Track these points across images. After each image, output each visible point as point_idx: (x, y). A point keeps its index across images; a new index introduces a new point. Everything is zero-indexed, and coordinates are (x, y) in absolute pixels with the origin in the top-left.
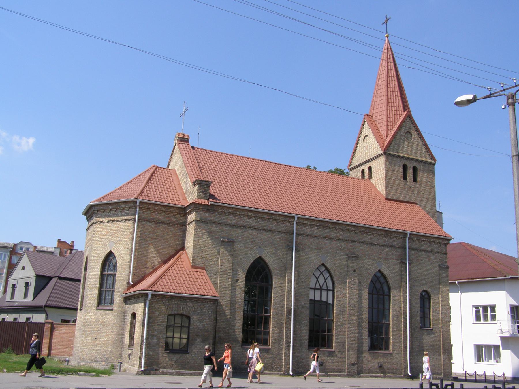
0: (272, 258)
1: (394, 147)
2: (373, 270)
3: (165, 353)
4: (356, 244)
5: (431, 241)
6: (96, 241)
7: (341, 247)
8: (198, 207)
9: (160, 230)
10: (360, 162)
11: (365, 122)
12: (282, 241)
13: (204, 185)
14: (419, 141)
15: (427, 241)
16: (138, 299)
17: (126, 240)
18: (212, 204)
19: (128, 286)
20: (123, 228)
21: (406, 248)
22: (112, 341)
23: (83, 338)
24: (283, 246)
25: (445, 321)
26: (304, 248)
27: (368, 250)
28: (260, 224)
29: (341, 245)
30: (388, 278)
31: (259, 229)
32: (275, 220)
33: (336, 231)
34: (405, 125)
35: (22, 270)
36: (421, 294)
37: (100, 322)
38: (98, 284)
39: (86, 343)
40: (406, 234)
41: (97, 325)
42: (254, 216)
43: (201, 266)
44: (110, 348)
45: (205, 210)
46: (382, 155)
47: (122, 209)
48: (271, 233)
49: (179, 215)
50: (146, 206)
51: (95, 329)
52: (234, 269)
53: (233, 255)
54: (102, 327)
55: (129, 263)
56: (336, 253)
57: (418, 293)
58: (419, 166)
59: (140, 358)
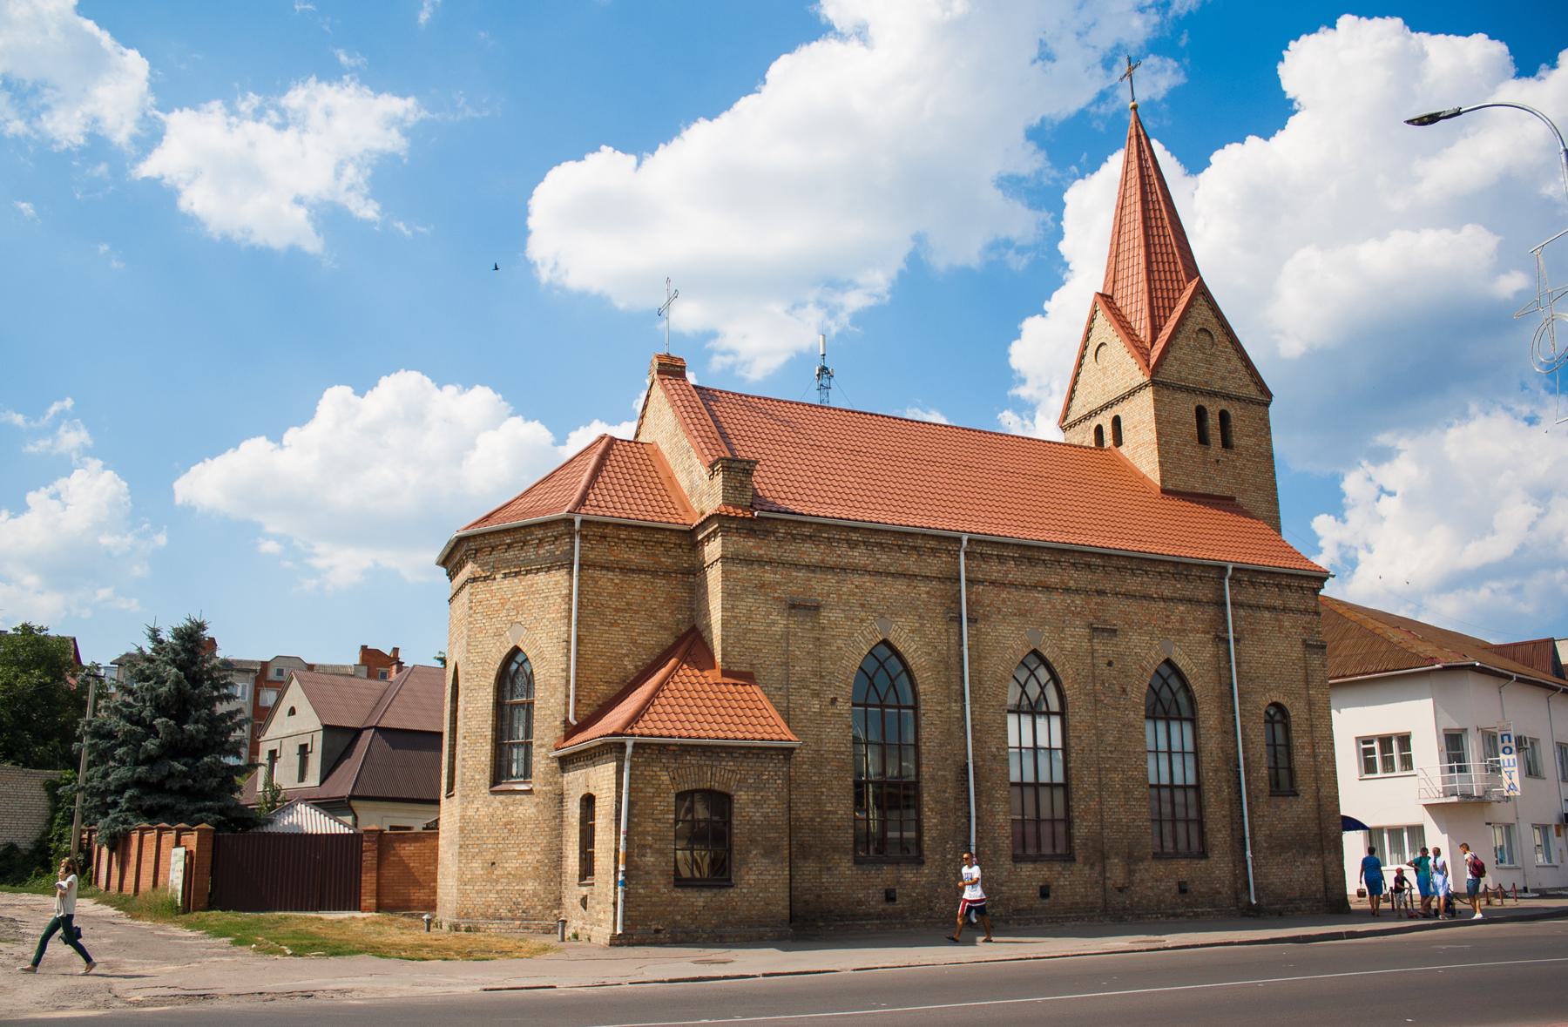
0: (913, 641)
1: (1171, 366)
2: (1153, 659)
3: (676, 889)
4: (1109, 599)
5: (1281, 584)
6: (478, 625)
7: (1073, 609)
8: (726, 525)
9: (635, 587)
10: (1089, 409)
11: (1096, 311)
12: (933, 600)
13: (737, 470)
14: (1230, 350)
15: (1274, 584)
16: (597, 759)
17: (553, 618)
18: (761, 515)
19: (565, 731)
20: (544, 587)
21: (1225, 604)
22: (533, 867)
23: (462, 865)
24: (937, 611)
26: (986, 613)
27: (1137, 611)
28: (878, 559)
29: (1073, 602)
30: (1188, 677)
31: (878, 573)
32: (914, 548)
33: (1060, 570)
34: (1194, 312)
35: (289, 715)
36: (1267, 712)
37: (501, 823)
38: (490, 729)
39: (469, 876)
40: (1224, 569)
41: (495, 831)
42: (864, 542)
43: (744, 669)
44: (530, 884)
45: (745, 531)
46: (1146, 386)
47: (537, 541)
48: (906, 580)
49: (680, 550)
50: (596, 530)
51: (491, 841)
52: (824, 674)
53: (819, 639)
54: (507, 835)
55: (565, 674)
56: (1064, 622)
57: (1260, 709)
58: (1234, 411)
59: (615, 904)
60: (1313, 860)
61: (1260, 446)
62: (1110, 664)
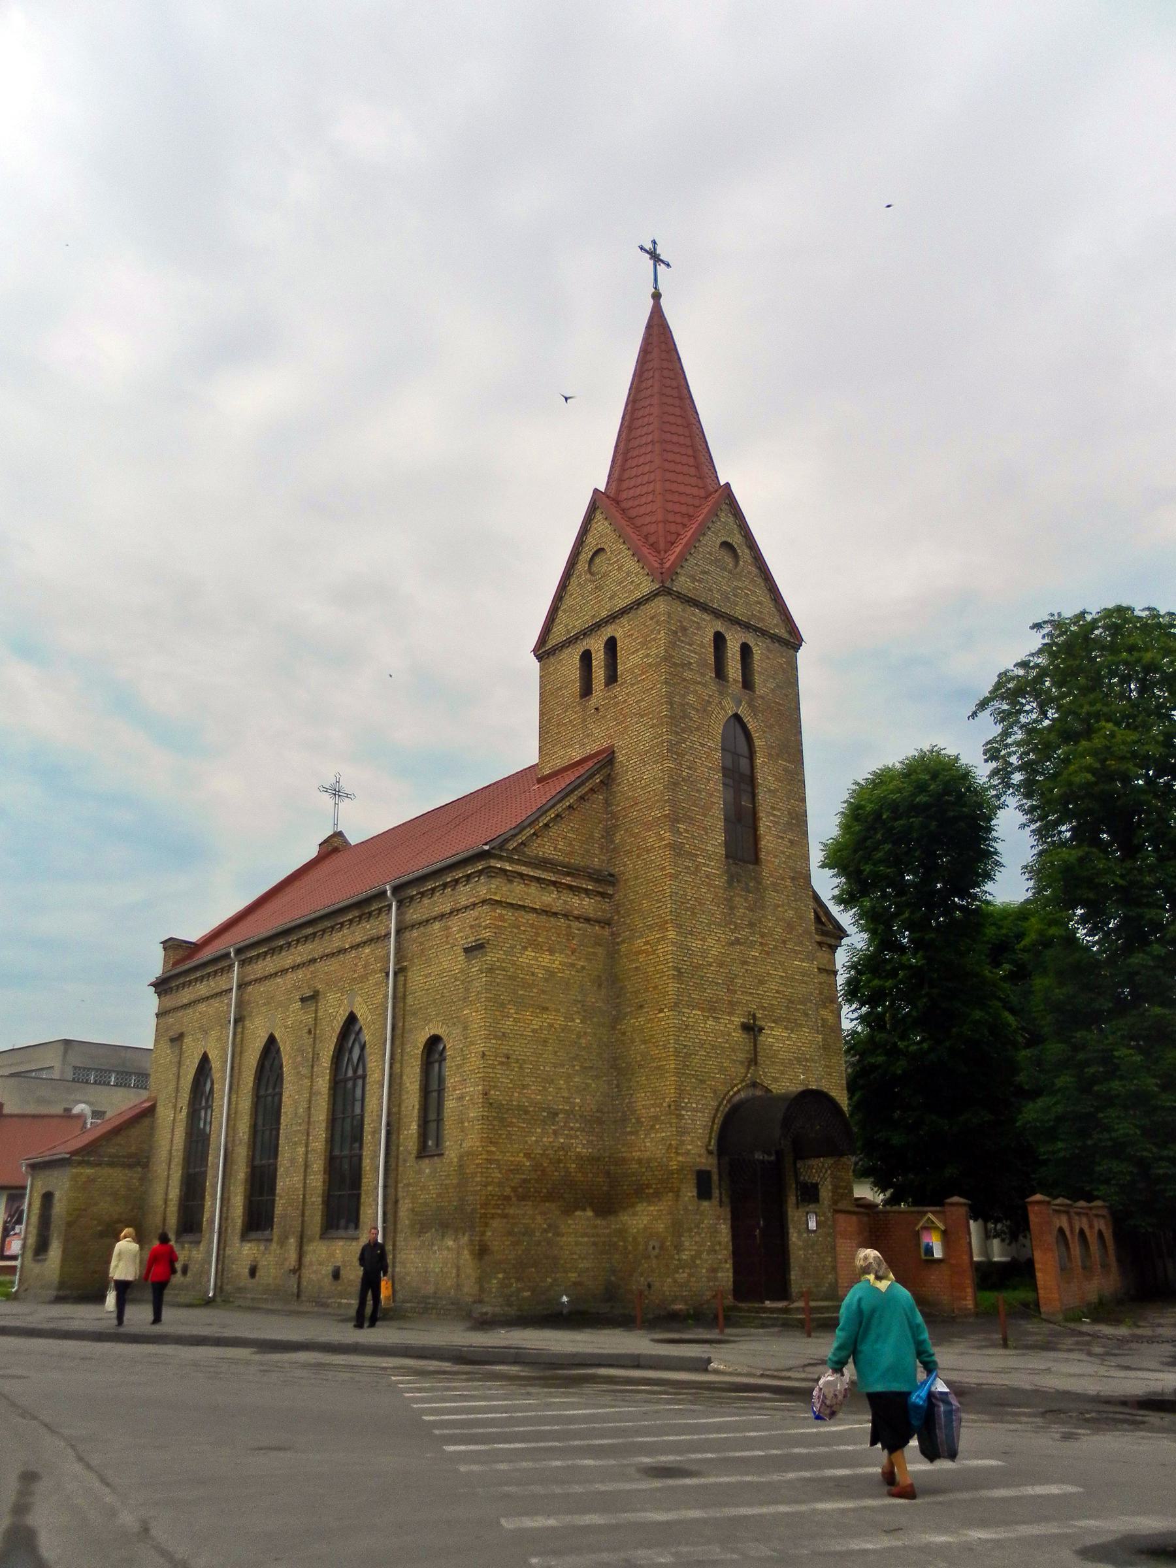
25: (469, 1122)
60: (450, 1243)
61: (648, 655)
62: (310, 1032)
